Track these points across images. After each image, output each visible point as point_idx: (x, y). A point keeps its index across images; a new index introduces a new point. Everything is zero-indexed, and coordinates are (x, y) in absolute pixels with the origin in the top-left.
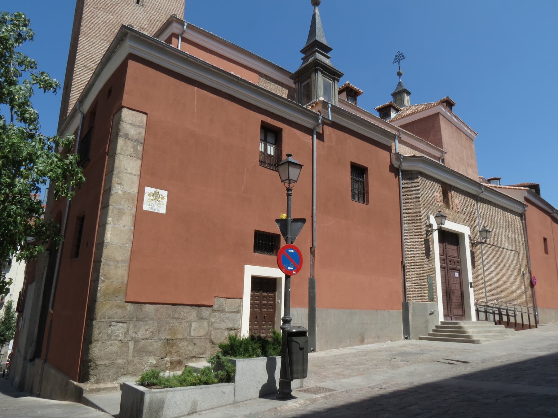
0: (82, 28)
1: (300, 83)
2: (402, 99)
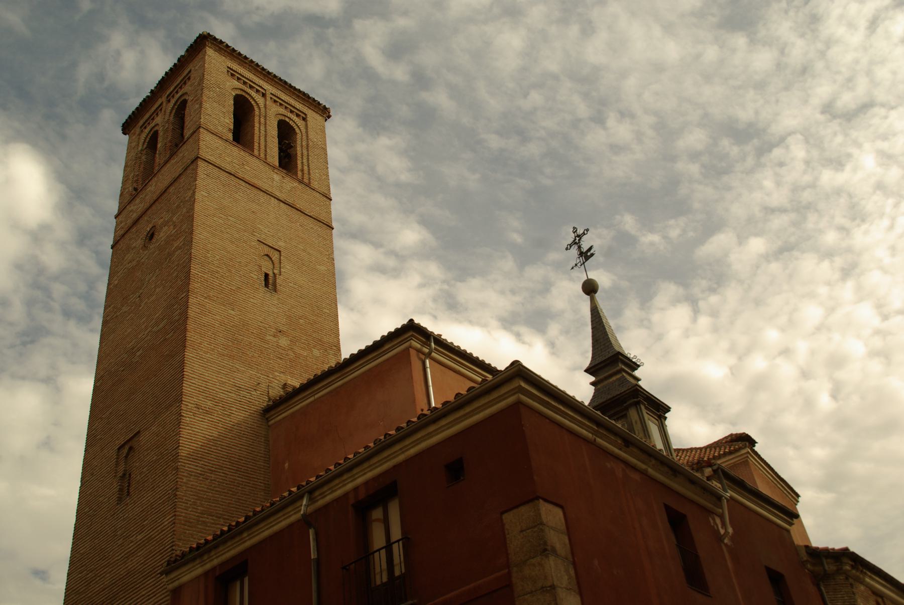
0: (188, 334)
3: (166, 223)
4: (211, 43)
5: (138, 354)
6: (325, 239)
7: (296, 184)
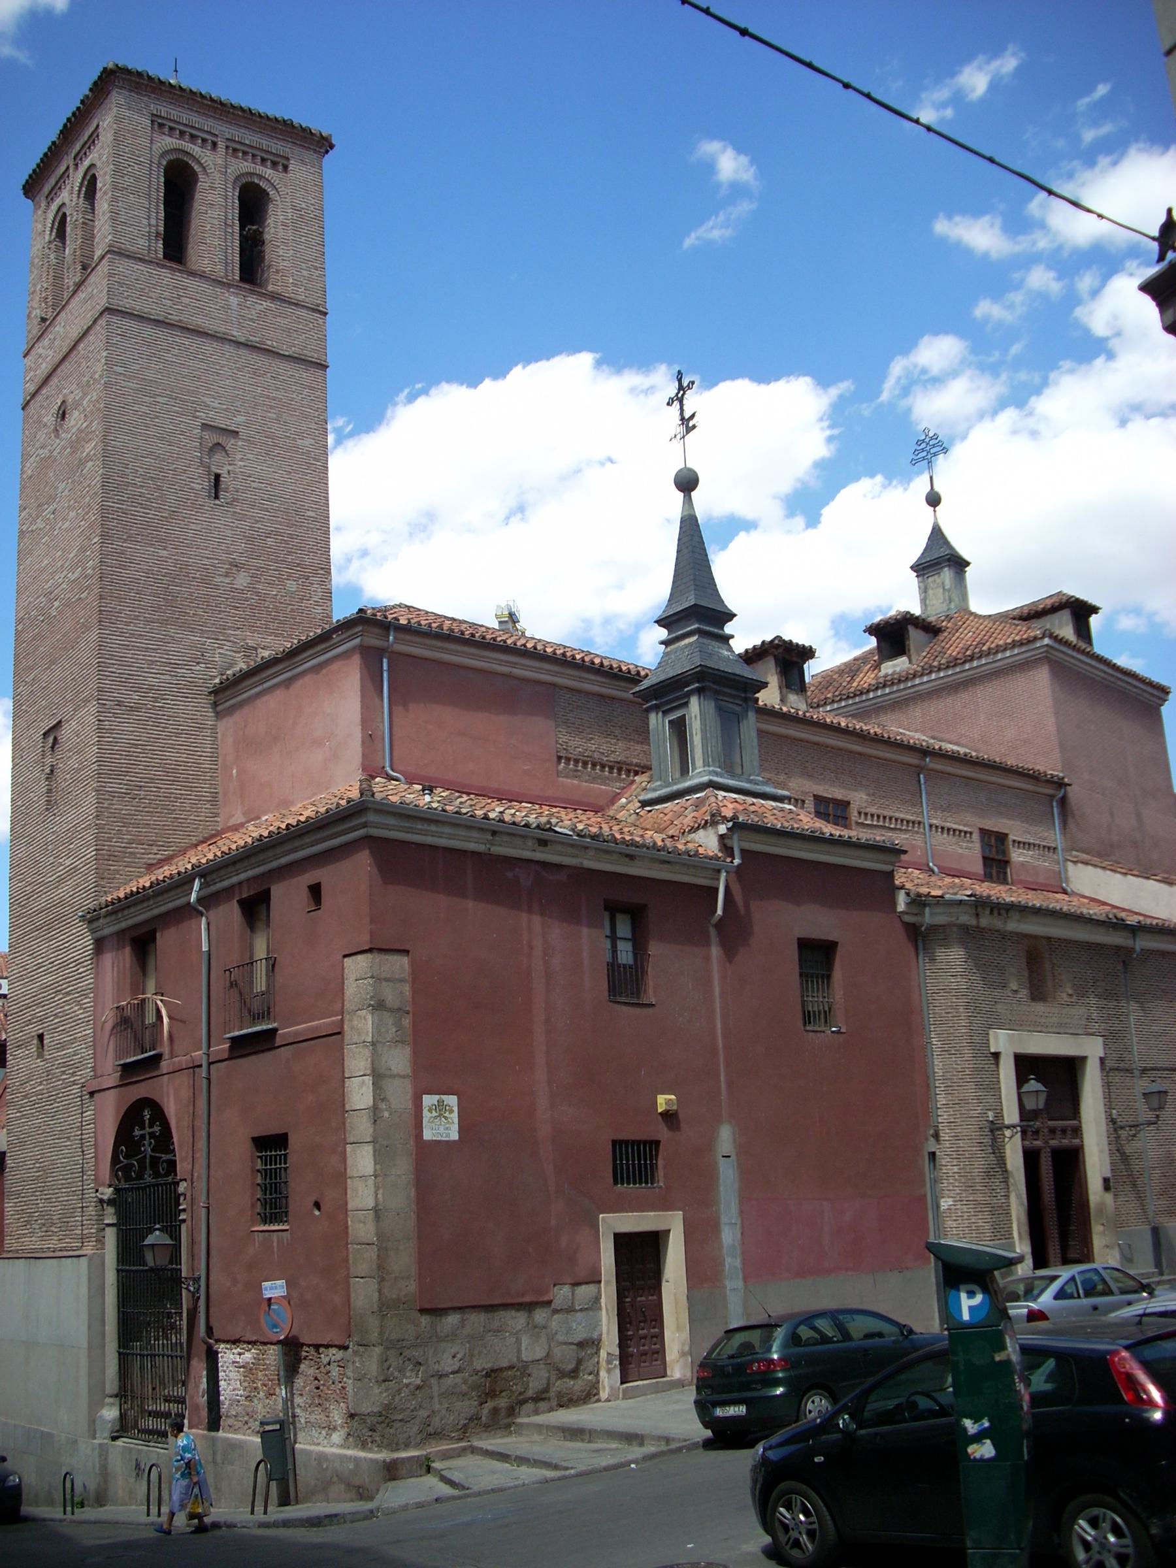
1: (660, 714)
2: (943, 583)
3: (77, 404)
4: (124, 79)
5: (56, 604)
6: (312, 389)
7: (266, 304)
